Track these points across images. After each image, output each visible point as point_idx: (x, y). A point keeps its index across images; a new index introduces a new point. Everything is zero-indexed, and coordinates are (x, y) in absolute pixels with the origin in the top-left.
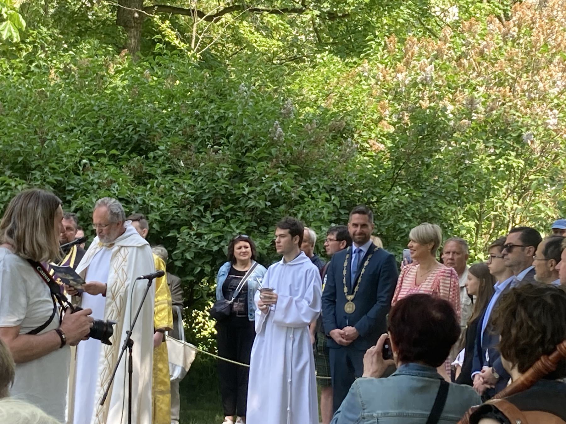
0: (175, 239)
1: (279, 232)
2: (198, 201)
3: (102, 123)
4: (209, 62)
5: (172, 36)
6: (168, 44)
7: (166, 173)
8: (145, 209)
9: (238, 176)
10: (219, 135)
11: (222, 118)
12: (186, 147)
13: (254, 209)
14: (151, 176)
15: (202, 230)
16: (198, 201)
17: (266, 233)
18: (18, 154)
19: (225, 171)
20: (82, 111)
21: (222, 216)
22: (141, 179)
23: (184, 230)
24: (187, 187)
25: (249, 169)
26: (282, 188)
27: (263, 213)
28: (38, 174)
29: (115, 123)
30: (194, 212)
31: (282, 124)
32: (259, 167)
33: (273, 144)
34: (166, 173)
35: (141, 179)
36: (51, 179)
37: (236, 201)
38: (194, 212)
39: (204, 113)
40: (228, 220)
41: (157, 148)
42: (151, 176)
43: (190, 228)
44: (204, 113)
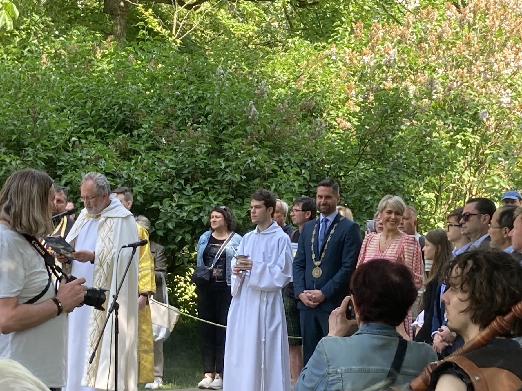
0: (158, 210)
1: (254, 203)
2: (178, 176)
3: (89, 104)
4: (188, 47)
5: (155, 24)
6: (151, 31)
7: (149, 149)
8: (130, 183)
9: (216, 151)
10: (198, 114)
11: (201, 99)
12: (167, 126)
13: (230, 182)
14: (136, 152)
15: (183, 202)
16: (178, 176)
17: (242, 204)
18: (12, 132)
19: (203, 148)
20: (72, 92)
21: (201, 189)
22: (126, 155)
23: (167, 202)
24: (169, 162)
25: (226, 145)
26: (256, 162)
27: (239, 186)
28: (30, 150)
29: (102, 103)
30: (176, 185)
31: (256, 103)
32: (236, 143)
33: (248, 122)
34: (149, 149)
35: (126, 155)
36: (42, 155)
37: (214, 175)
38: (176, 185)
39: (184, 94)
40: (206, 192)
41: (140, 126)
42: (136, 152)
43: (172, 199)
44: (184, 94)
